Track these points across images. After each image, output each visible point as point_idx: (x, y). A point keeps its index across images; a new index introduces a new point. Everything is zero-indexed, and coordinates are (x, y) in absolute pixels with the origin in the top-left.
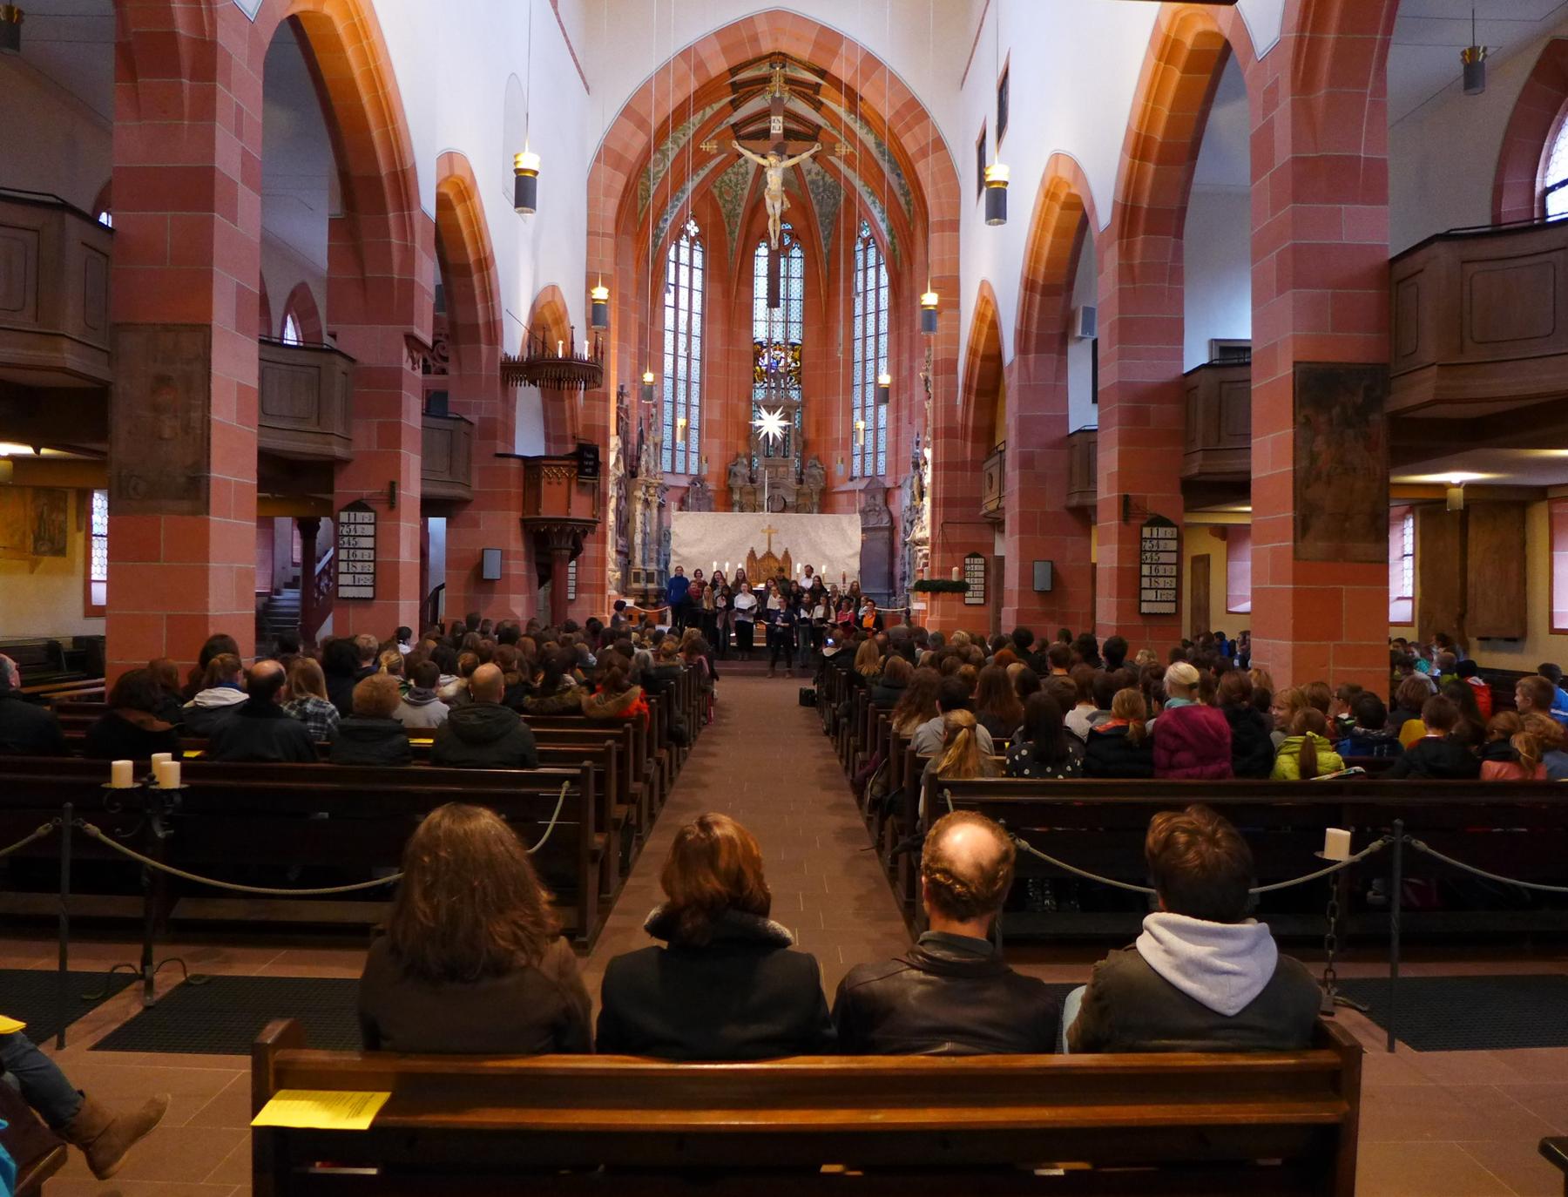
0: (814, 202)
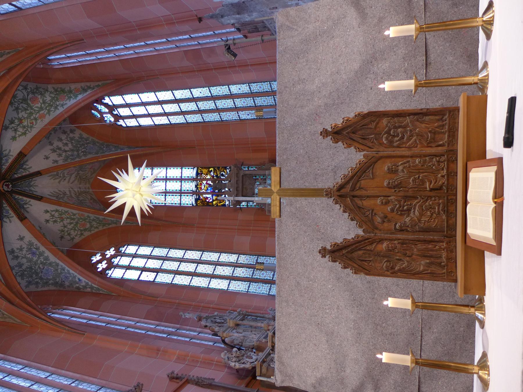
0: (83, 158)
